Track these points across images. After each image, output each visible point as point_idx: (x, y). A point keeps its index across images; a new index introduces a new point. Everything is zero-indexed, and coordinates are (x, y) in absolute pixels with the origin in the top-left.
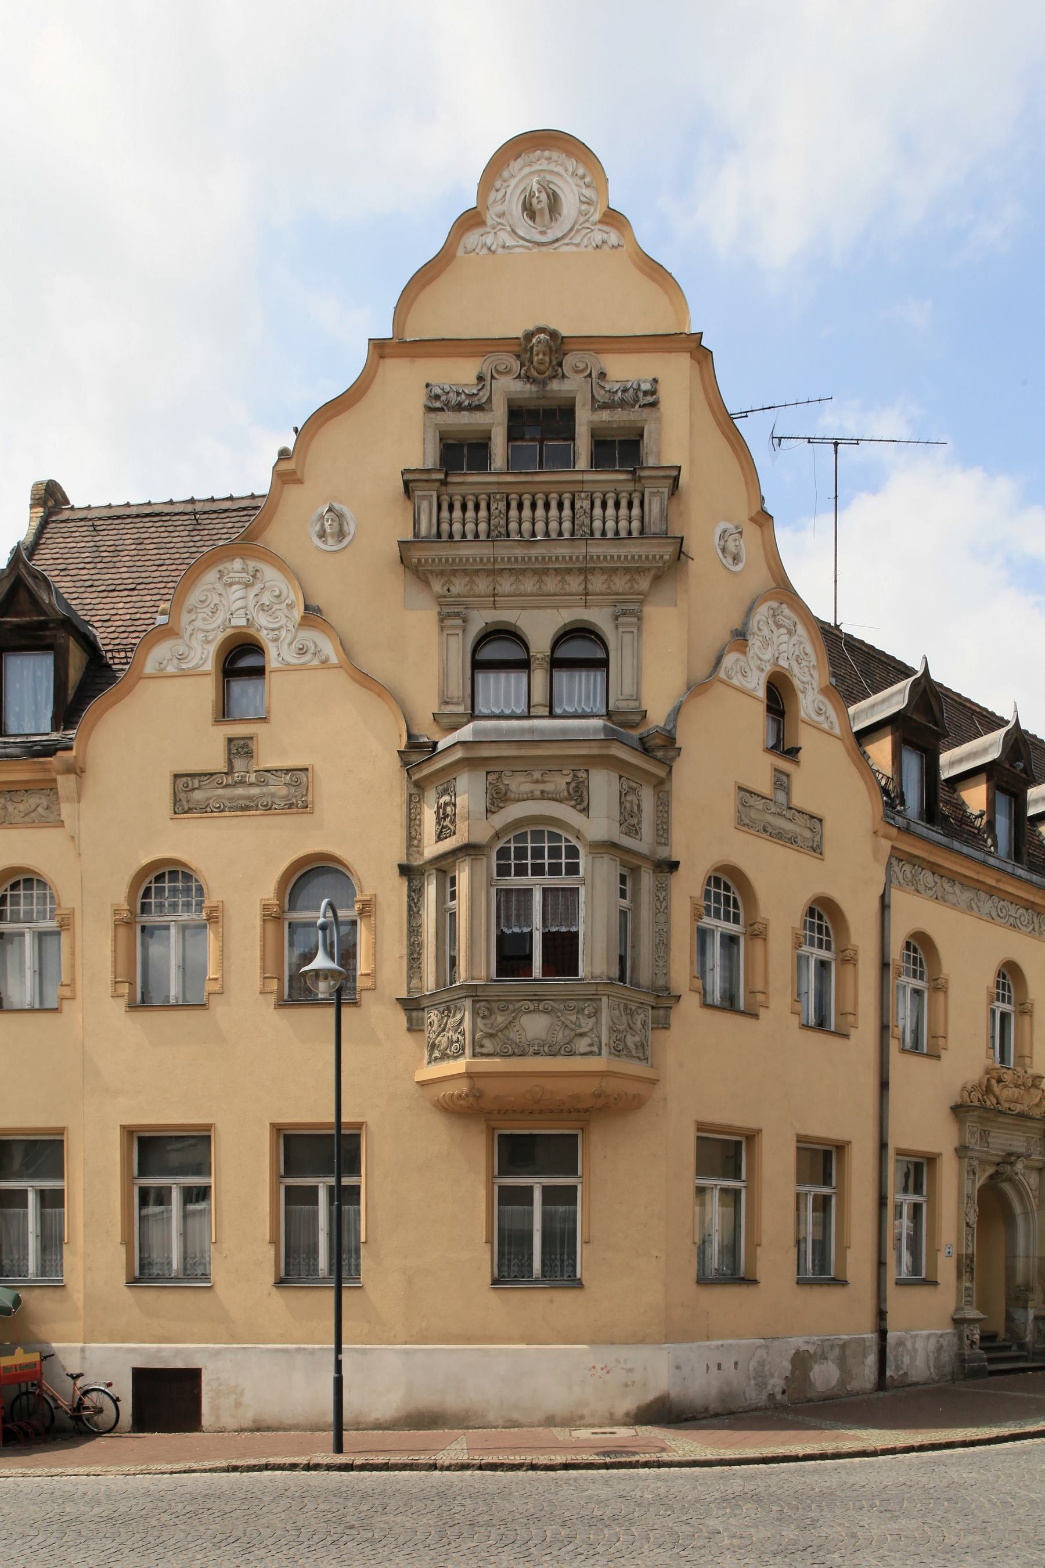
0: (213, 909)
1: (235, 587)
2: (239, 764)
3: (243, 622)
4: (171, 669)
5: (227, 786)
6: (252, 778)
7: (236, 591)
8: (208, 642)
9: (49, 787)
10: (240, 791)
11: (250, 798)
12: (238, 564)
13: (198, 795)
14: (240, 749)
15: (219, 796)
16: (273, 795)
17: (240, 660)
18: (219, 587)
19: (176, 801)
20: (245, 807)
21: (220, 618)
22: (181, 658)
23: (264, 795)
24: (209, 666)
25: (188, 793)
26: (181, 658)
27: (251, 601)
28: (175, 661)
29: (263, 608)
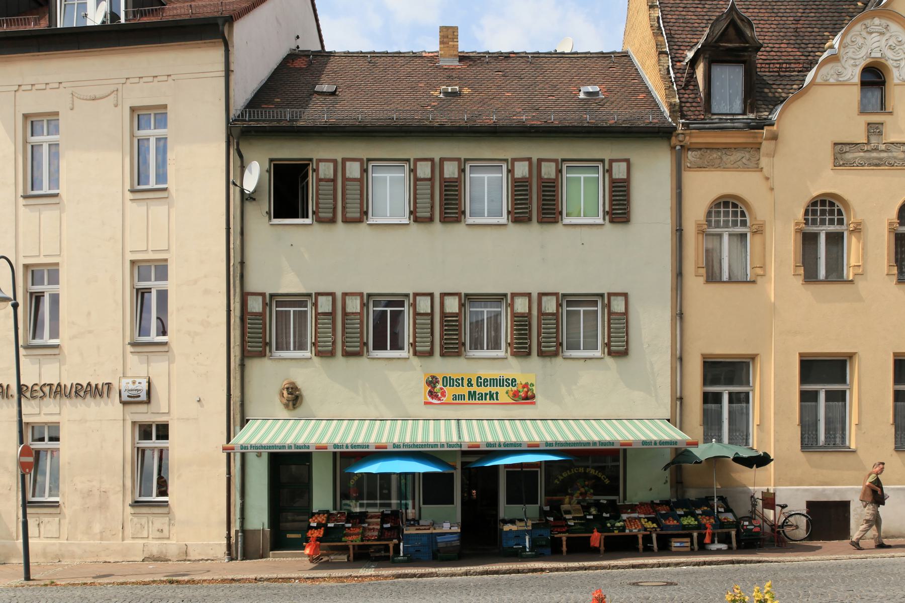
0: (859, 224)
1: (874, 35)
2: (874, 140)
3: (879, 55)
4: (832, 81)
5: (867, 151)
6: (883, 147)
7: (875, 37)
8: (856, 65)
9: (757, 147)
10: (874, 155)
11: (880, 159)
12: (877, 21)
13: (849, 156)
14: (874, 129)
15: (862, 157)
16: (895, 158)
17: (874, 77)
18: (864, 34)
19: (835, 159)
20: (878, 164)
21: (863, 52)
22: (839, 74)
23: (889, 157)
24: (857, 79)
25: (842, 154)
26: (839, 74)
27: (883, 42)
28: (835, 76)
29: (890, 47)
